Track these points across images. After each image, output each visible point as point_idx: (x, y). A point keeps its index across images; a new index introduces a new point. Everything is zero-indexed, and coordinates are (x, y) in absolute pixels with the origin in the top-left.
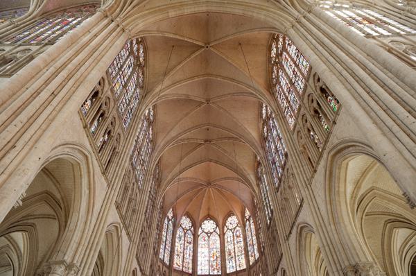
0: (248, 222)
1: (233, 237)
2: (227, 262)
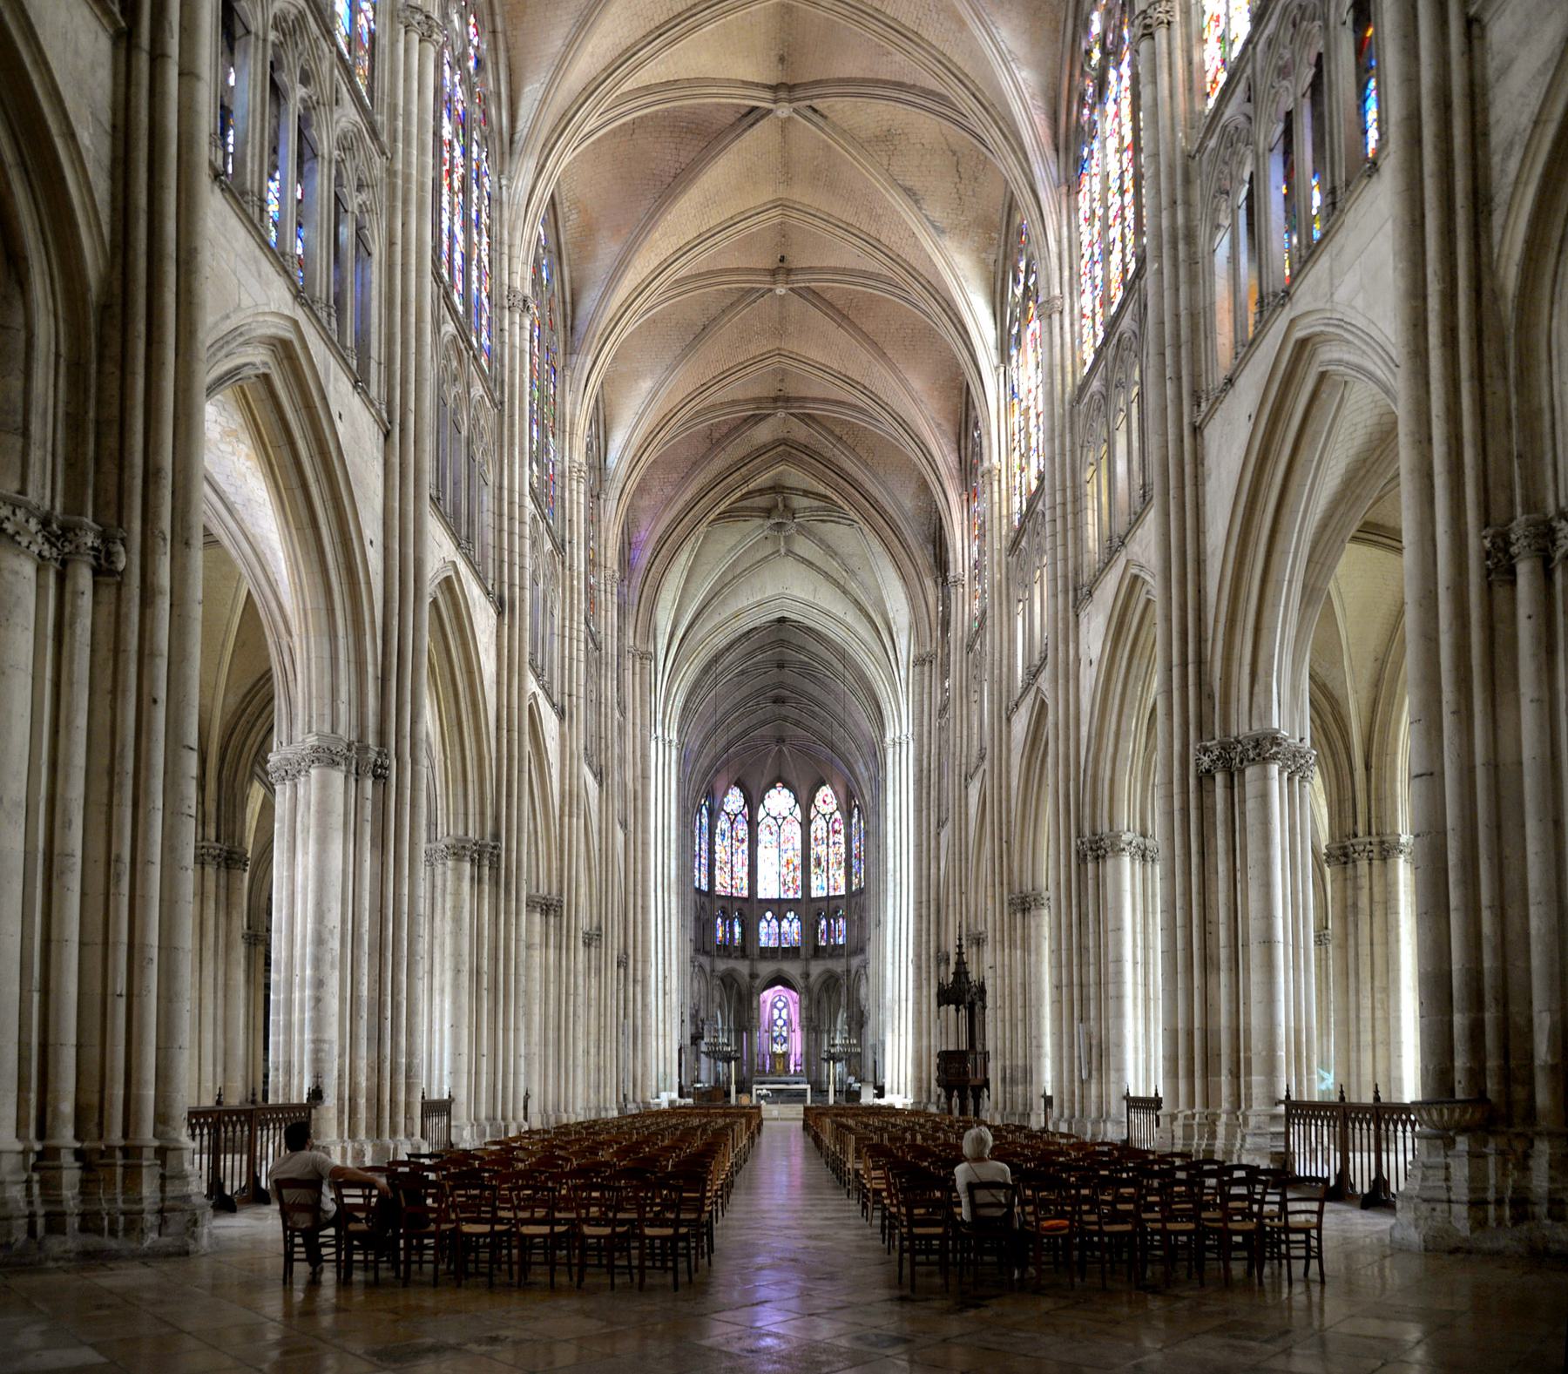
0: (856, 811)
2: (813, 877)
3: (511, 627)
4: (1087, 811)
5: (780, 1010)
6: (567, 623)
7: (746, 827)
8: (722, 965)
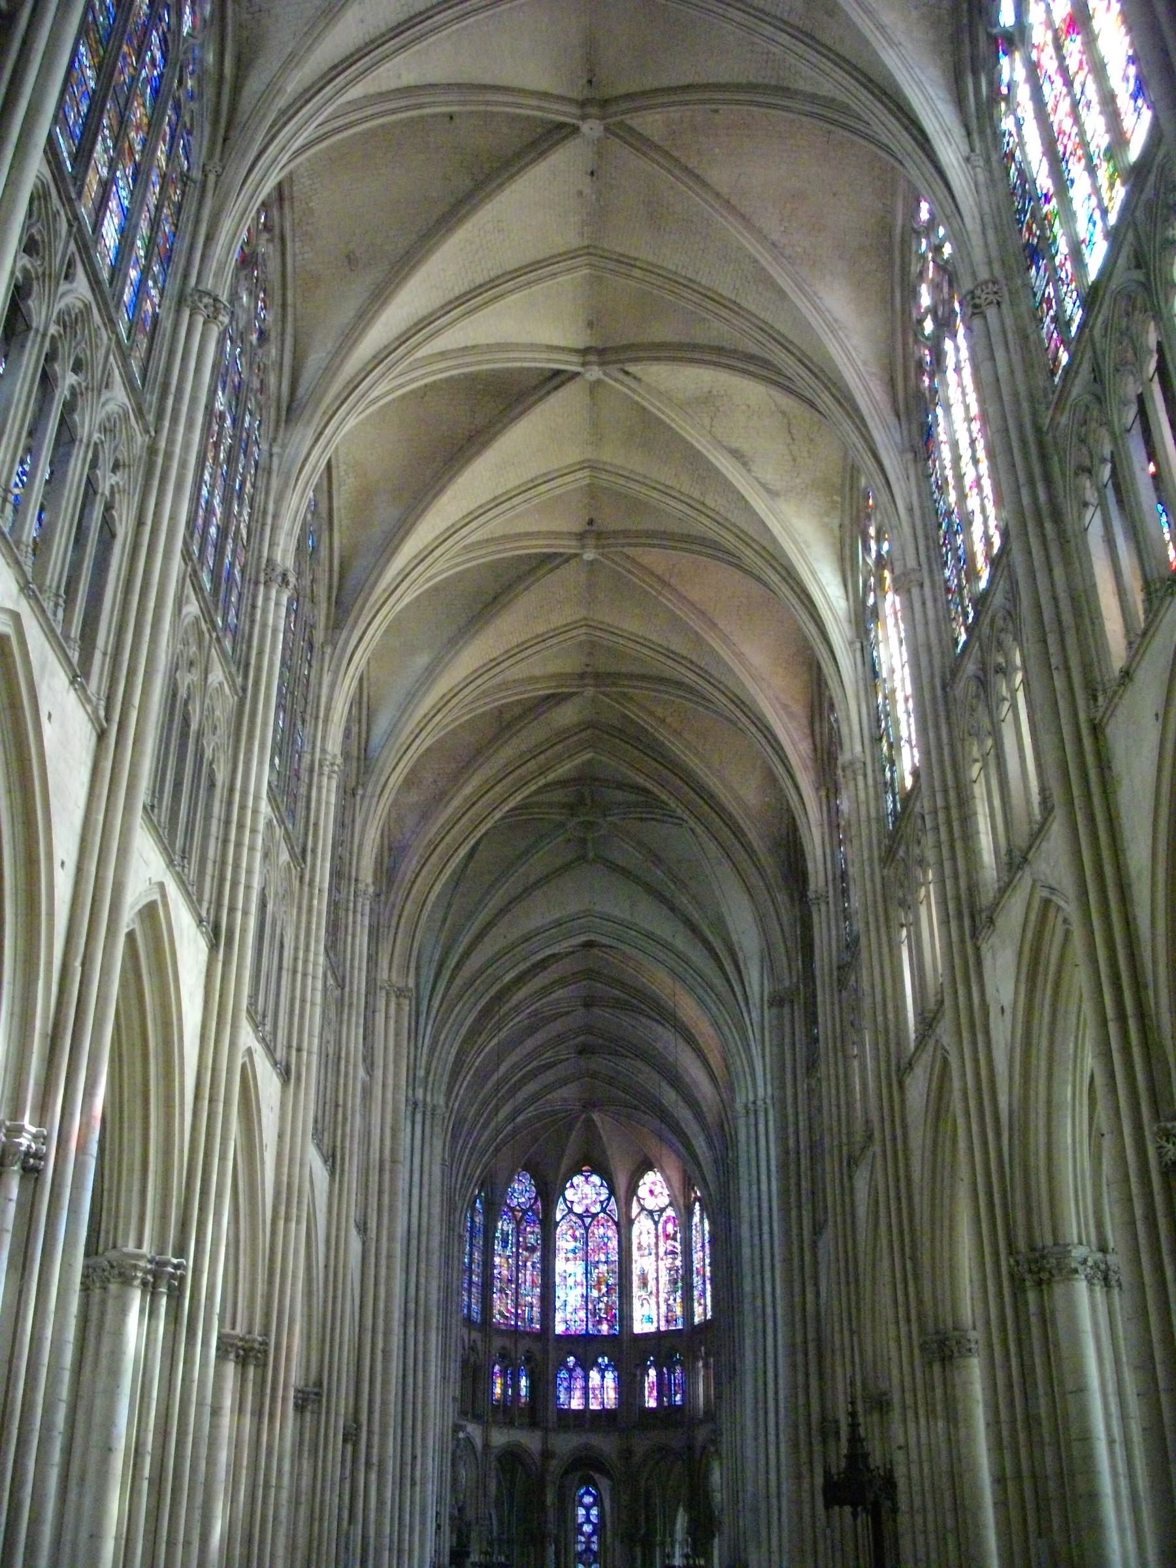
1: (657, 1237)
3: (226, 963)
4: (1020, 1215)
5: (588, 1508)
6: (301, 954)
7: (537, 1230)
8: (500, 1438)
